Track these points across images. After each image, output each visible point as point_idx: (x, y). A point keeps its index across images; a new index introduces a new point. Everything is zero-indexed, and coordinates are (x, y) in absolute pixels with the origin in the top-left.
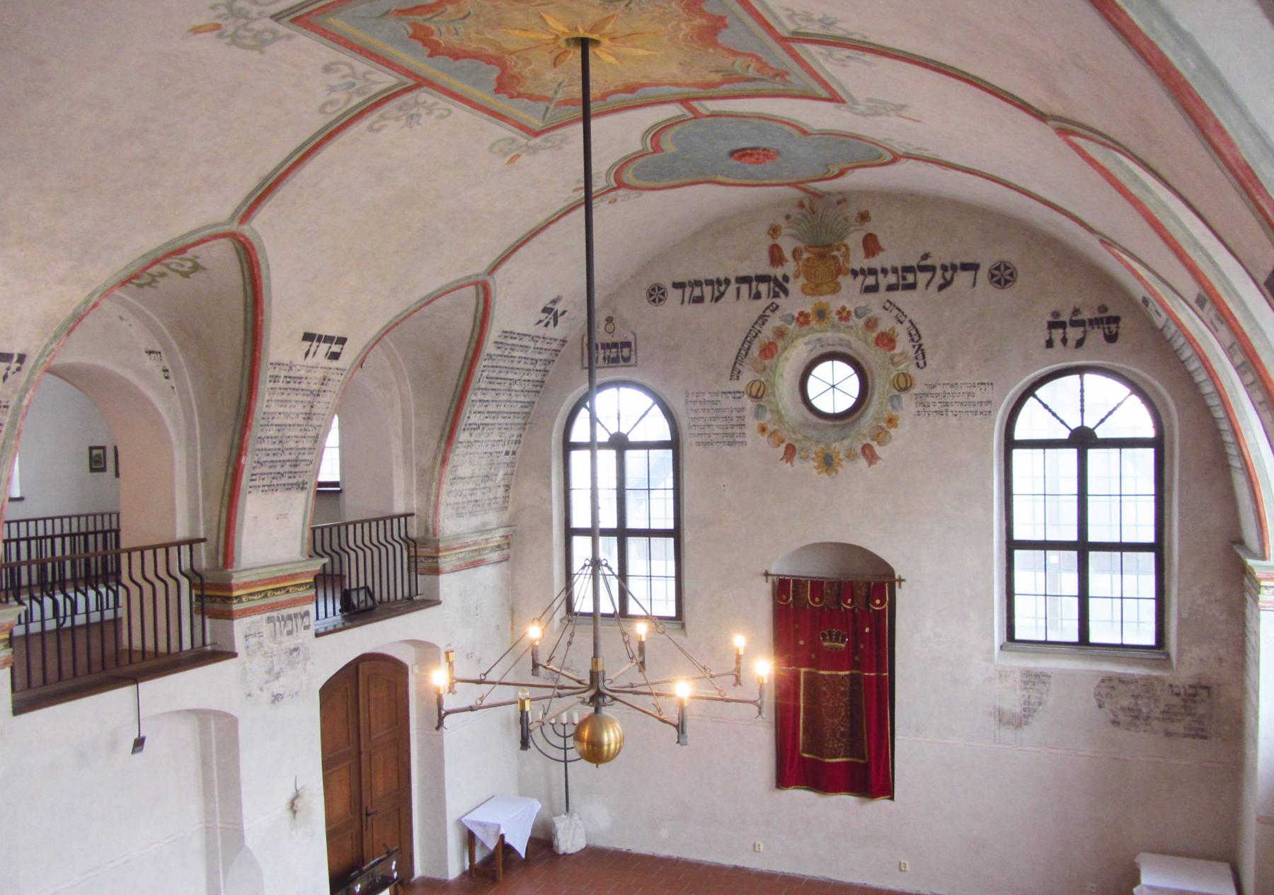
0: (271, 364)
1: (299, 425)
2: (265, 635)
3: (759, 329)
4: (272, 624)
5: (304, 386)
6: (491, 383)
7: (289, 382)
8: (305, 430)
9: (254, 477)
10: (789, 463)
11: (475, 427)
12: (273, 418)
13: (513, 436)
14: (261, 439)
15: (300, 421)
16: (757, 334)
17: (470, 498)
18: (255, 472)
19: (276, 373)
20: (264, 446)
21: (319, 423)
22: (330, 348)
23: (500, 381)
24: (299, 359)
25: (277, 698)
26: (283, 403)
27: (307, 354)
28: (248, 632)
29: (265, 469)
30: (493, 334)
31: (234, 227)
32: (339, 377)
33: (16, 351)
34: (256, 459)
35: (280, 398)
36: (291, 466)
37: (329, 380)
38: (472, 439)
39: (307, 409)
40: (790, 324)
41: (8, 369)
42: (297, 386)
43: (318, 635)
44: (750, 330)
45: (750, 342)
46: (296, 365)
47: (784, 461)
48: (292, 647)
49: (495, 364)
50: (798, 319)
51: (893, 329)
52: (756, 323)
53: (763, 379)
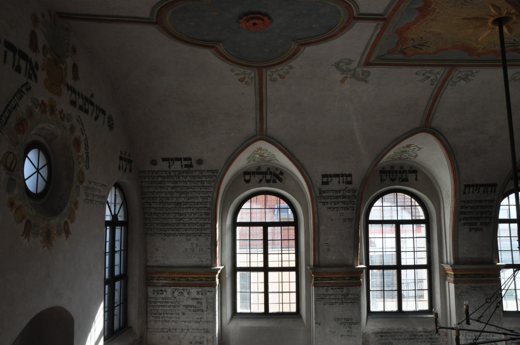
3: (18, 102)
10: (27, 239)
16: (15, 106)
40: (37, 108)
44: (11, 100)
45: (10, 112)
47: (24, 236)
50: (40, 104)
51: (80, 137)
52: (15, 95)
53: (16, 153)
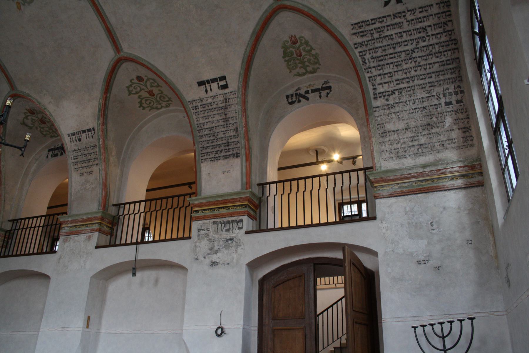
0: (189, 102)
1: (222, 125)
2: (211, 230)
4: (216, 225)
5: (214, 106)
6: (381, 60)
7: (204, 107)
8: (226, 127)
9: (203, 155)
11: (387, 94)
12: (204, 125)
13: (448, 89)
14: (202, 137)
15: (223, 123)
17: (411, 144)
18: (203, 152)
19: (194, 105)
20: (204, 139)
21: (235, 122)
22: (218, 84)
23: (391, 56)
24: (203, 94)
25: (214, 264)
26: (207, 117)
27: (206, 91)
28: (200, 228)
29: (209, 150)
30: (345, 32)
31: (118, 56)
32: (234, 96)
33: (91, 127)
34: (201, 146)
35: (204, 115)
36: (225, 146)
37: (229, 99)
38: (391, 102)
39: (224, 117)
41: (92, 134)
42: (210, 107)
43: (247, 232)
46: (204, 99)
48: (229, 238)
49: (371, 47)
